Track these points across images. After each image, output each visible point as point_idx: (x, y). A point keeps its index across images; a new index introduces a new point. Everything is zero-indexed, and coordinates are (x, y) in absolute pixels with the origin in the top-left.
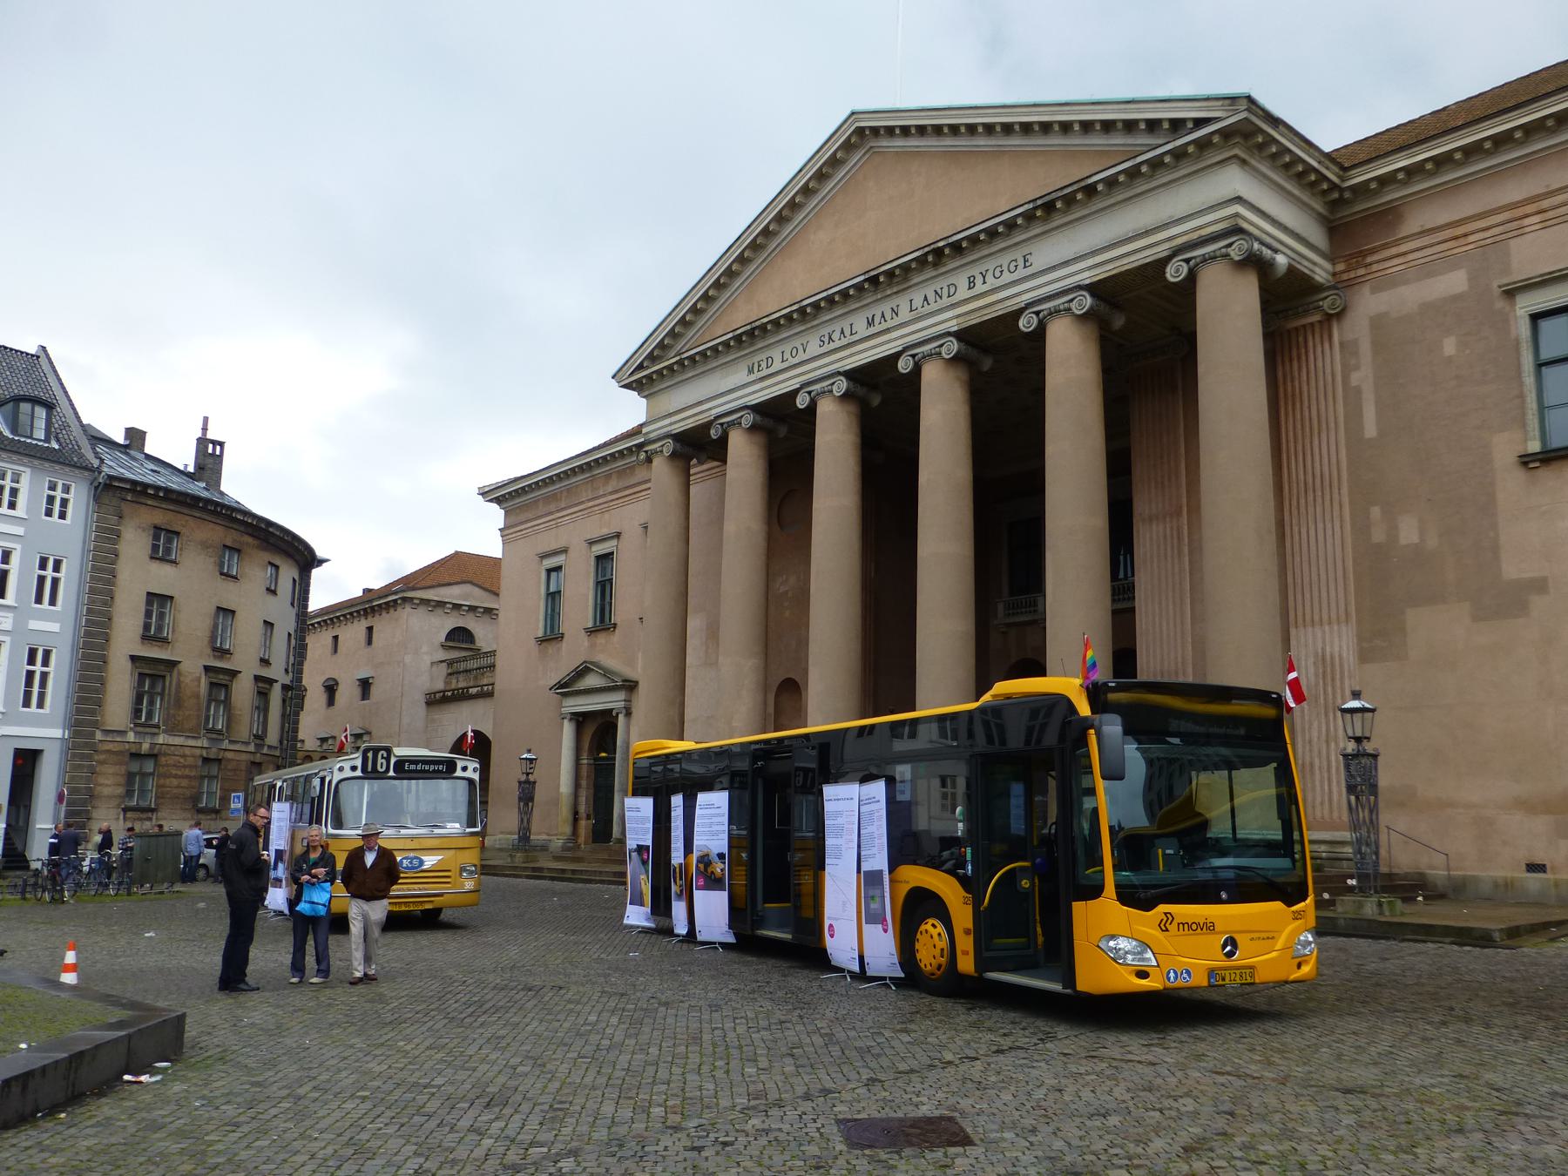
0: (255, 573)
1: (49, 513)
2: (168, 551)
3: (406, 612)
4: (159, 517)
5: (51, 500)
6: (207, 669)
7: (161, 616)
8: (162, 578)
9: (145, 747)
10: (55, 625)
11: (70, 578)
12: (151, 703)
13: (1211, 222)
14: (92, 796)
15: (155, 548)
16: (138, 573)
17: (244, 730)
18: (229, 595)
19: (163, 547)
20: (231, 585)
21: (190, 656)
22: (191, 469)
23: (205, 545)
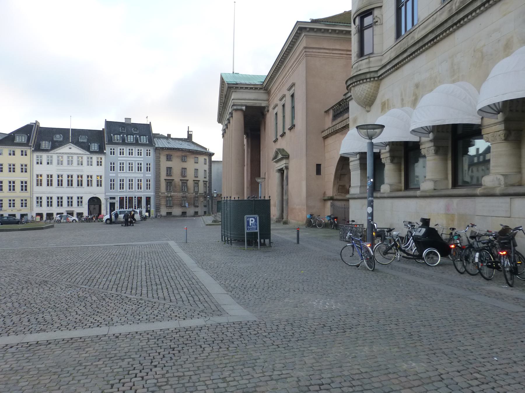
1: (147, 155)
2: (170, 159)
5: (147, 153)
6: (181, 180)
7: (170, 171)
8: (169, 164)
9: (169, 195)
10: (150, 175)
12: (170, 187)
14: (160, 204)
15: (167, 159)
16: (164, 164)
17: (191, 190)
18: (184, 165)
19: (169, 158)
20: (185, 163)
21: (176, 177)
22: (186, 137)
23: (178, 157)
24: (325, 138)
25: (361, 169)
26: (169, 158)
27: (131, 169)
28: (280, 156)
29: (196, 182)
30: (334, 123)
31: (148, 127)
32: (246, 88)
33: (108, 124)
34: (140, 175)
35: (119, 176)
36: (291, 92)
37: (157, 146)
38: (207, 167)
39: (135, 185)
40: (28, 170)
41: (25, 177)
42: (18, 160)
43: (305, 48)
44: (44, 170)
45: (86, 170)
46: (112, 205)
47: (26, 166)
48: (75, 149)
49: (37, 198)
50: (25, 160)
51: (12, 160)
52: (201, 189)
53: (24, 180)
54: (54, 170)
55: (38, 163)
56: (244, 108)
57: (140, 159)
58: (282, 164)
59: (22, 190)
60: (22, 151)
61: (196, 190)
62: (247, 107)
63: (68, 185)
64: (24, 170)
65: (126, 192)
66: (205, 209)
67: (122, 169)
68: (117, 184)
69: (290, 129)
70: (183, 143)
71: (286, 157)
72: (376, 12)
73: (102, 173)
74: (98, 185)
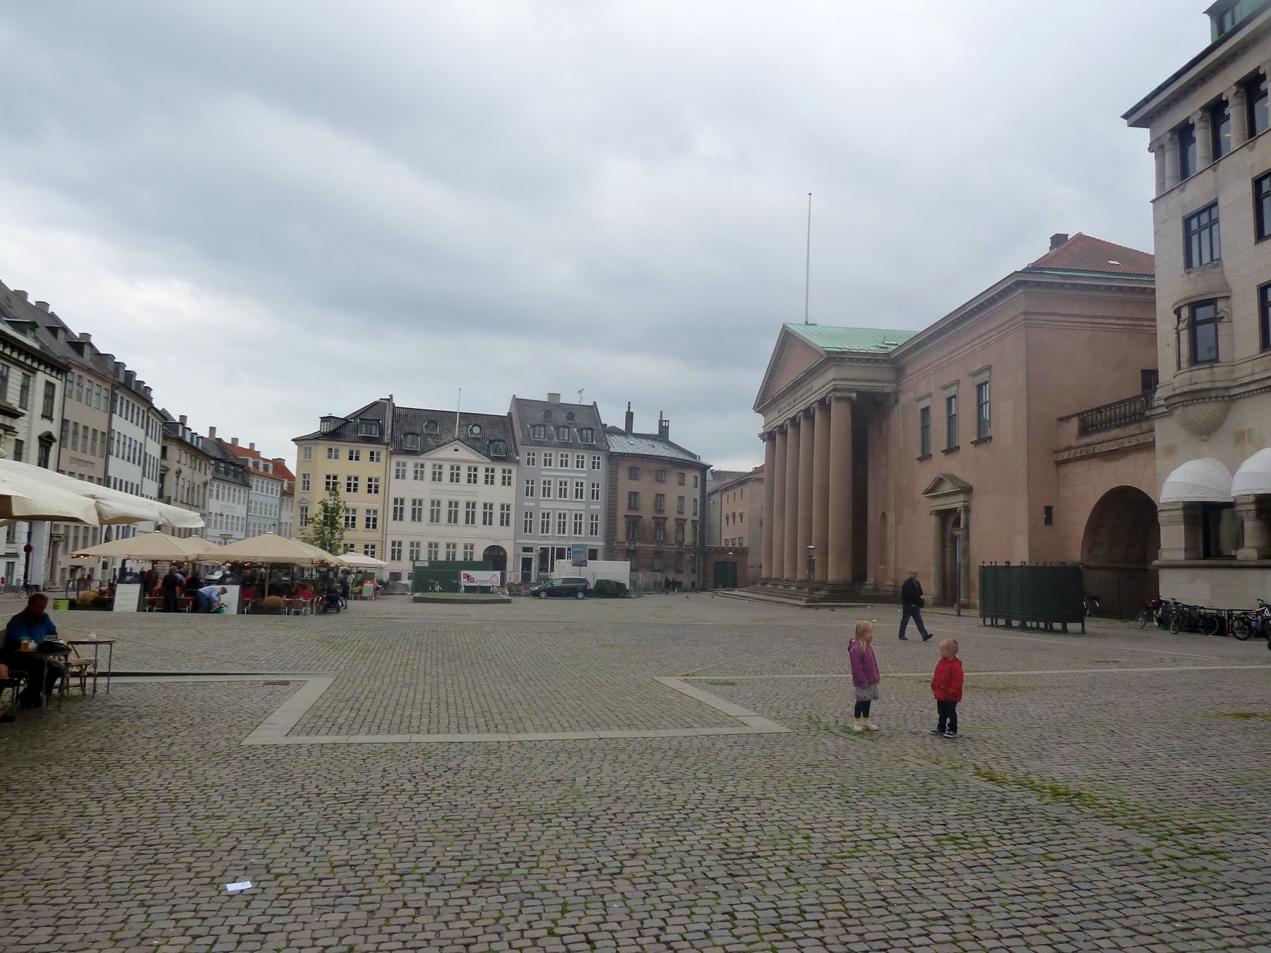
0: (672, 479)
3: (749, 484)
4: (630, 463)
8: (634, 486)
10: (598, 507)
11: (602, 490)
13: (830, 386)
16: (626, 485)
17: (672, 540)
18: (662, 489)
19: (634, 474)
24: (1060, 463)
25: (1186, 523)
26: (634, 474)
27: (563, 493)
28: (947, 487)
29: (680, 523)
30: (1085, 440)
31: (593, 409)
32: (859, 360)
33: (518, 403)
34: (579, 506)
35: (542, 506)
36: (980, 379)
37: (612, 450)
38: (697, 494)
39: (570, 526)
40: (381, 489)
41: (374, 501)
42: (364, 469)
43: (1025, 313)
44: (406, 489)
45: (483, 493)
46: (527, 563)
47: (377, 480)
48: (466, 455)
49: (394, 544)
50: (376, 469)
51: (353, 468)
52: (689, 539)
53: (372, 506)
54: (424, 490)
55: (397, 477)
56: (854, 395)
57: (582, 475)
58: (956, 502)
59: (368, 526)
60: (372, 454)
61: (680, 539)
62: (858, 393)
63: (450, 521)
64: (372, 488)
65: (553, 538)
66: (694, 578)
67: (546, 492)
68: (538, 522)
69: (976, 443)
70: (655, 444)
71: (967, 490)
72: (1220, 305)
73: (511, 501)
74: (502, 524)
